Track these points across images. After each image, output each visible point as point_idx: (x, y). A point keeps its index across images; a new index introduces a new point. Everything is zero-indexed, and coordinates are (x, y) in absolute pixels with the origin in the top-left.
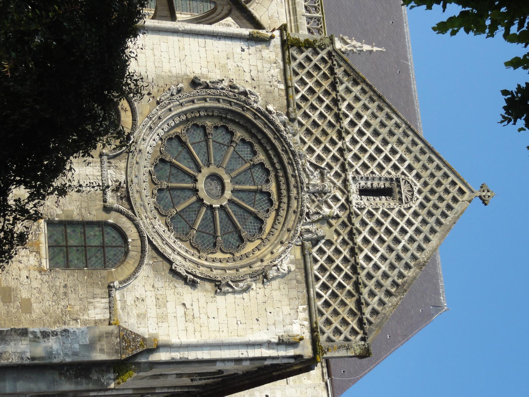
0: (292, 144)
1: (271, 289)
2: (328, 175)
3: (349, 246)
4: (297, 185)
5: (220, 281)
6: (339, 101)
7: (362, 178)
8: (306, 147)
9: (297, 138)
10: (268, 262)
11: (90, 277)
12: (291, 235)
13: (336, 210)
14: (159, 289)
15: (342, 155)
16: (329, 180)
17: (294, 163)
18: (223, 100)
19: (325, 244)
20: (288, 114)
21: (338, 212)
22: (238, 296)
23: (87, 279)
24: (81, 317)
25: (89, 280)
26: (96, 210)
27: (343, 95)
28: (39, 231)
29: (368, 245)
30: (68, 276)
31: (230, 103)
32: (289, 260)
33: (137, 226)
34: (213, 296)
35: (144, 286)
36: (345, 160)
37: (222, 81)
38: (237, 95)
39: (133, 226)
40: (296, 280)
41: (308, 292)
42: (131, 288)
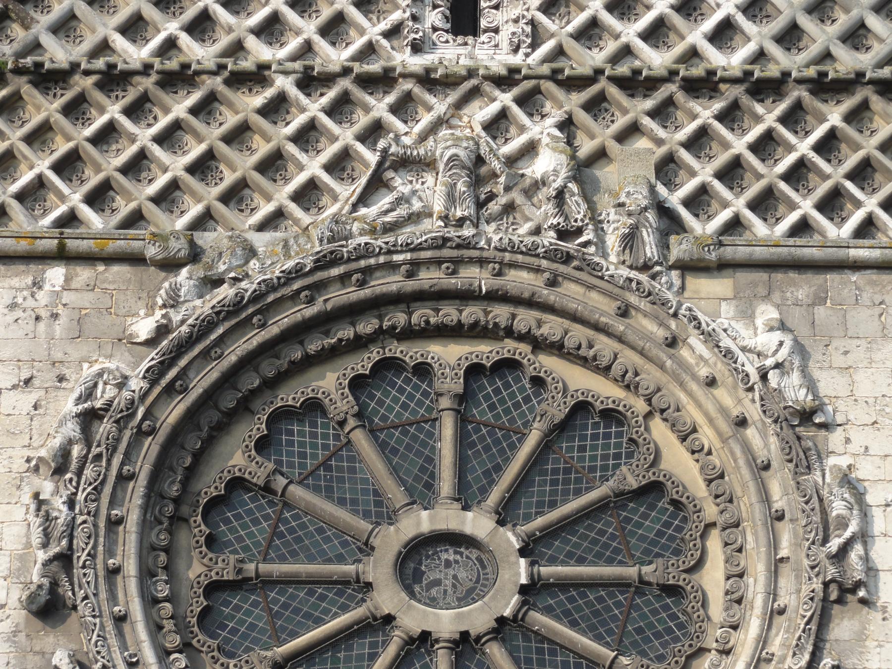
0: (290, 264)
1: (850, 401)
2: (407, 140)
3: (680, 97)
4: (451, 260)
5: (826, 585)
6: (111, 66)
7: (415, 18)
8: (294, 209)
9: (260, 240)
10: (747, 402)
12: (644, 304)
13: (542, 129)
15: (328, 79)
16: (430, 142)
17: (363, 263)
18: (112, 504)
19: (671, 185)
20: (170, 265)
21: (549, 121)
22: (878, 525)
27: (87, 46)
29: (673, 28)
31: (123, 479)
32: (750, 327)
34: (879, 616)
36: (346, 71)
37: (40, 502)
38: (95, 451)
40: (813, 304)
41: (857, 266)
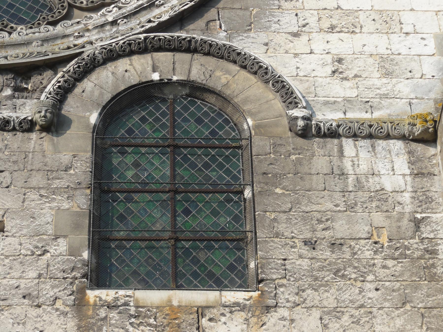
11: (277, 179)
14: (304, 22)
23: (283, 188)
24: (408, 209)
25: (286, 183)
26: (56, 150)
28: (126, 304)
30: (277, 235)
33: (111, 55)
35: (296, 55)
39: (111, 66)
42: (306, 85)
